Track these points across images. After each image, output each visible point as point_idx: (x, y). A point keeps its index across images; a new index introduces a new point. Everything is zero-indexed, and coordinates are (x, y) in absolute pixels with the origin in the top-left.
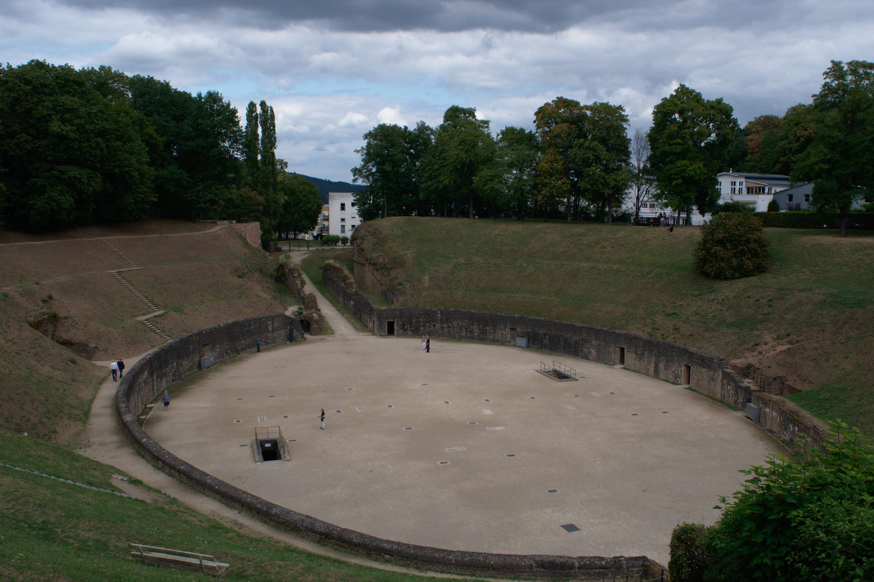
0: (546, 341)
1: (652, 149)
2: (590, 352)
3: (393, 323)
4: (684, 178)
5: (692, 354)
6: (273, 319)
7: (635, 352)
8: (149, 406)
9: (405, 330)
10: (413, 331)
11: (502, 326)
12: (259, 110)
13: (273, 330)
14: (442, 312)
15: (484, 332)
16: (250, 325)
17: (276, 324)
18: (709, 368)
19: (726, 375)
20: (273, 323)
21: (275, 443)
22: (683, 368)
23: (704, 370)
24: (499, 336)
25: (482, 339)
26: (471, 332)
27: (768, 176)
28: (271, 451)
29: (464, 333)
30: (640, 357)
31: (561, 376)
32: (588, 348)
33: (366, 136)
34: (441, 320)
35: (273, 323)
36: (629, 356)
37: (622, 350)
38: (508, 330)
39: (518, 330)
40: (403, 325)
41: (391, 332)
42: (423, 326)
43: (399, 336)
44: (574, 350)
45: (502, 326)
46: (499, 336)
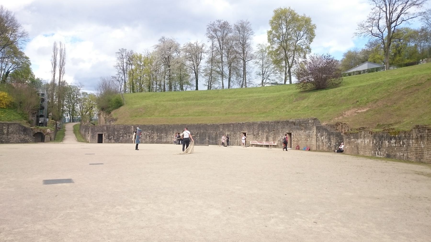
3: (102, 134)
9: (110, 139)
13: (8, 134)
15: (161, 138)
17: (11, 130)
20: (8, 128)
24: (169, 139)
26: (152, 138)
35: (8, 128)
40: (109, 136)
41: (100, 141)
42: (122, 136)
43: (105, 142)
45: (171, 132)
46: (169, 139)
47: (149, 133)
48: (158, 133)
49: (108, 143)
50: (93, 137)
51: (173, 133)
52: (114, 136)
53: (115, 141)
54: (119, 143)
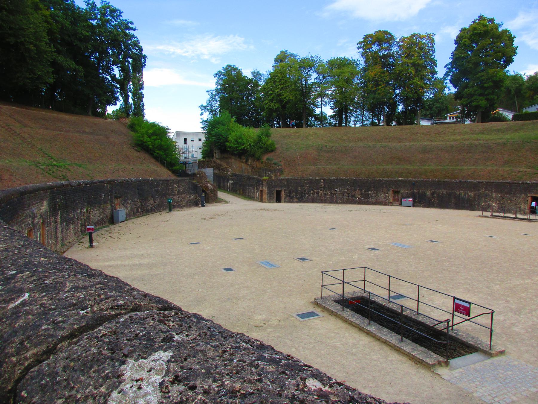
0: (435, 200)
4: (494, 82)
6: (178, 183)
9: (292, 198)
10: (298, 199)
11: (385, 189)
14: (324, 180)
16: (158, 186)
17: (181, 188)
20: (178, 186)
24: (382, 198)
25: (365, 200)
26: (353, 196)
29: (346, 198)
32: (485, 202)
34: (324, 188)
38: (391, 193)
39: (402, 191)
40: (290, 193)
41: (278, 200)
42: (308, 194)
43: (285, 202)
45: (385, 189)
47: (348, 189)
48: (361, 190)
49: (289, 202)
50: (270, 194)
51: (389, 190)
52: (296, 193)
53: (298, 200)
54: (304, 202)
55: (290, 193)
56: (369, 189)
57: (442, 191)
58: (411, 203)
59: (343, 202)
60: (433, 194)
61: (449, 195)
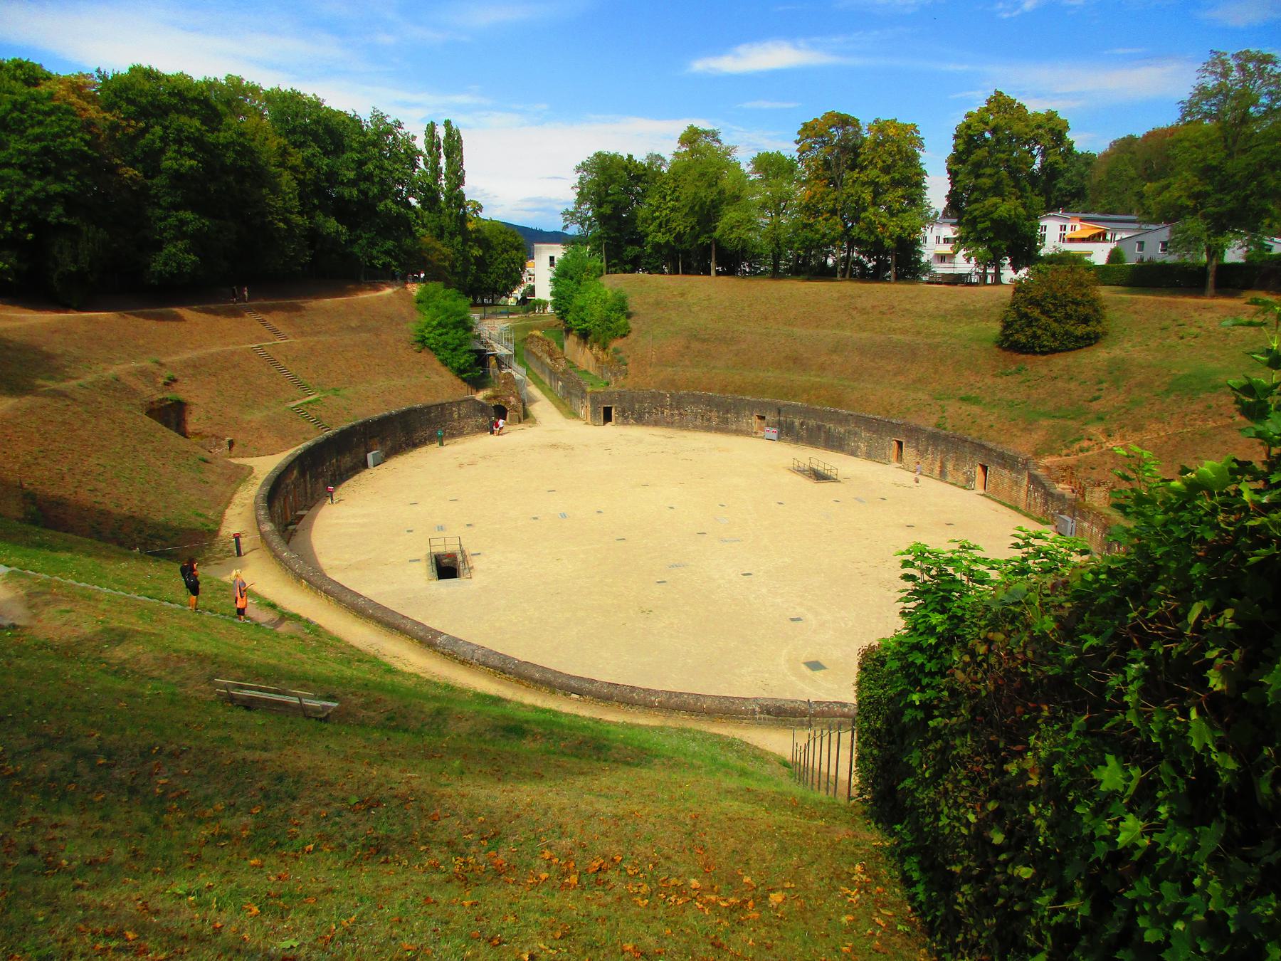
0: (804, 433)
1: (952, 184)
2: (858, 447)
4: (992, 220)
5: (991, 450)
7: (916, 447)
8: (300, 513)
9: (626, 418)
10: (636, 420)
12: (441, 132)
15: (725, 421)
16: (429, 413)
17: (464, 411)
18: (1012, 469)
19: (1034, 480)
21: (452, 556)
22: (979, 469)
23: (1005, 472)
24: (744, 426)
25: (723, 427)
26: (709, 420)
27: (1111, 217)
28: (446, 568)
29: (699, 422)
30: (922, 453)
31: (819, 476)
33: (578, 169)
36: (908, 453)
37: (900, 444)
38: (755, 418)
40: (624, 411)
41: (607, 418)
44: (835, 443)
46: (744, 426)
49: (623, 424)
55: (624, 411)
56: (728, 412)
57: (812, 423)
58: (774, 436)
59: (696, 428)
60: (802, 424)
61: (819, 428)
